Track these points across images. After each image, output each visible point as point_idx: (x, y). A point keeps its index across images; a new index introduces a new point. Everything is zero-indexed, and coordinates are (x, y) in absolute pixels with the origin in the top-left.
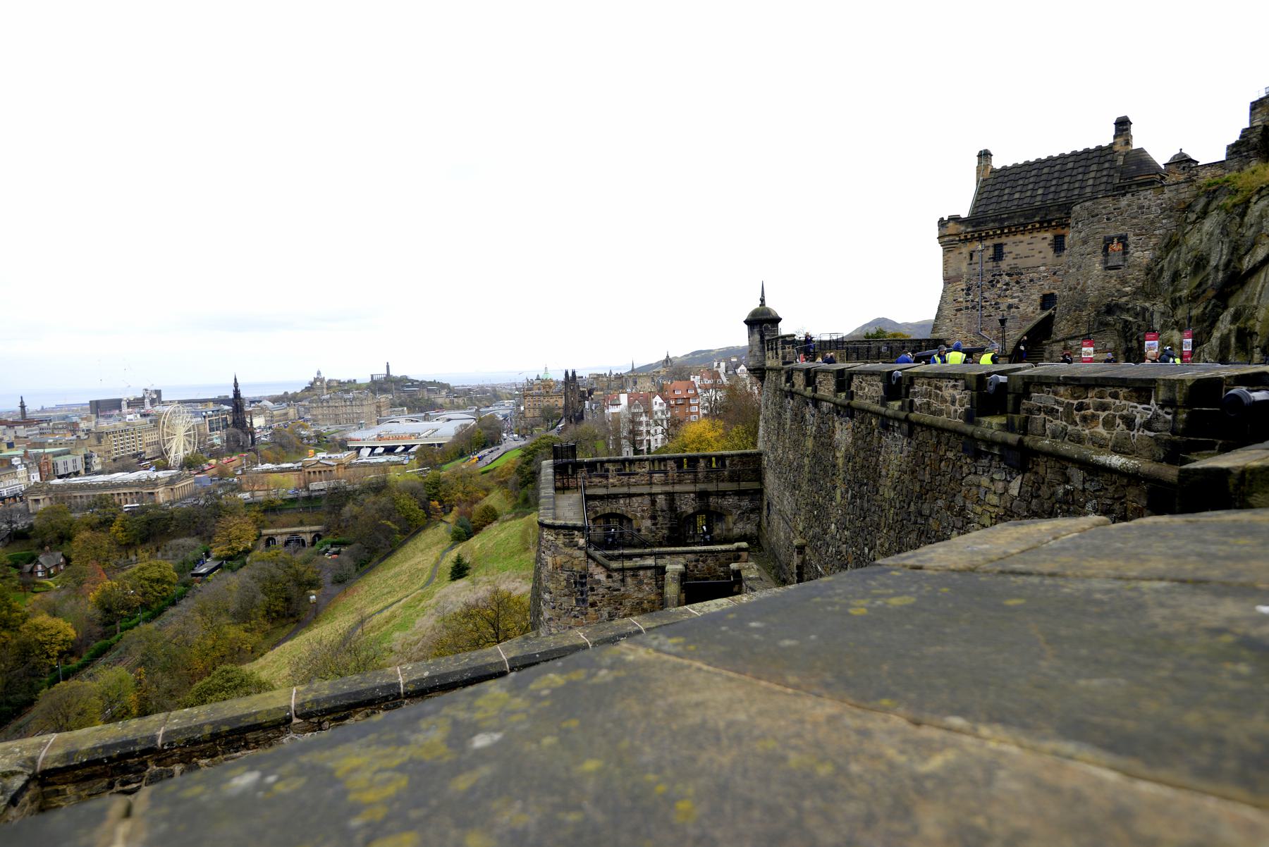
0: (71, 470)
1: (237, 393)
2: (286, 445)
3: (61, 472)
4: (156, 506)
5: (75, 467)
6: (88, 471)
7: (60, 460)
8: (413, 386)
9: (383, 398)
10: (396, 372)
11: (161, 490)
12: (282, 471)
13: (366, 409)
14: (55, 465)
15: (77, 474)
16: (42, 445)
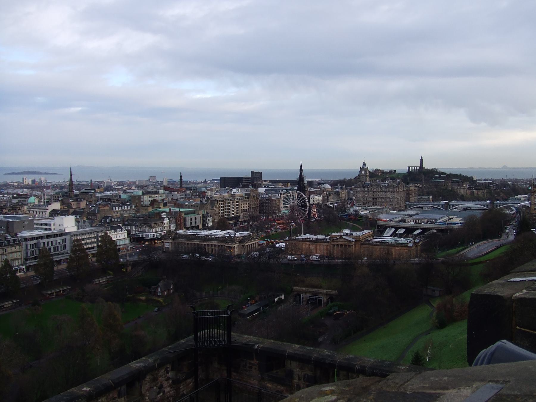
0: (194, 224)
1: (301, 177)
3: (188, 225)
4: (230, 257)
5: (196, 223)
6: (205, 227)
7: (188, 217)
8: (440, 178)
9: (411, 187)
10: (427, 166)
11: (236, 245)
12: (317, 241)
13: (396, 195)
14: (185, 220)
15: (193, 228)
16: (182, 206)
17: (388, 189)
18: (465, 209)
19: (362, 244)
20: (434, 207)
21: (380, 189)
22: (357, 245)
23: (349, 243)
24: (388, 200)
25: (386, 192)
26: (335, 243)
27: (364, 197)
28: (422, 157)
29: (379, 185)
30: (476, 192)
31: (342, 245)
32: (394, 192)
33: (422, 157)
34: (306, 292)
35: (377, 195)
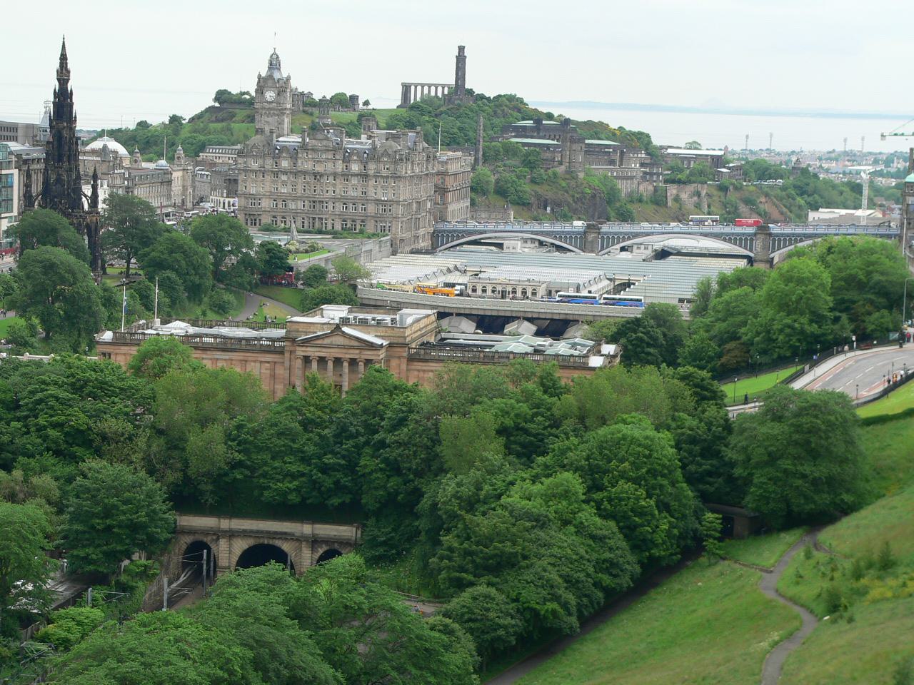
2: (220, 269)
9: (457, 162)
10: (483, 82)
12: (227, 345)
13: (405, 192)
17: (372, 168)
18: (662, 254)
19: (411, 359)
20: (541, 244)
21: (340, 167)
22: (394, 363)
23: (369, 354)
24: (371, 208)
25: (364, 176)
26: (313, 352)
27: (275, 197)
28: (461, 49)
29: (337, 148)
30: (672, 190)
31: (338, 362)
32: (397, 177)
33: (461, 49)
34: (231, 535)
35: (330, 188)
